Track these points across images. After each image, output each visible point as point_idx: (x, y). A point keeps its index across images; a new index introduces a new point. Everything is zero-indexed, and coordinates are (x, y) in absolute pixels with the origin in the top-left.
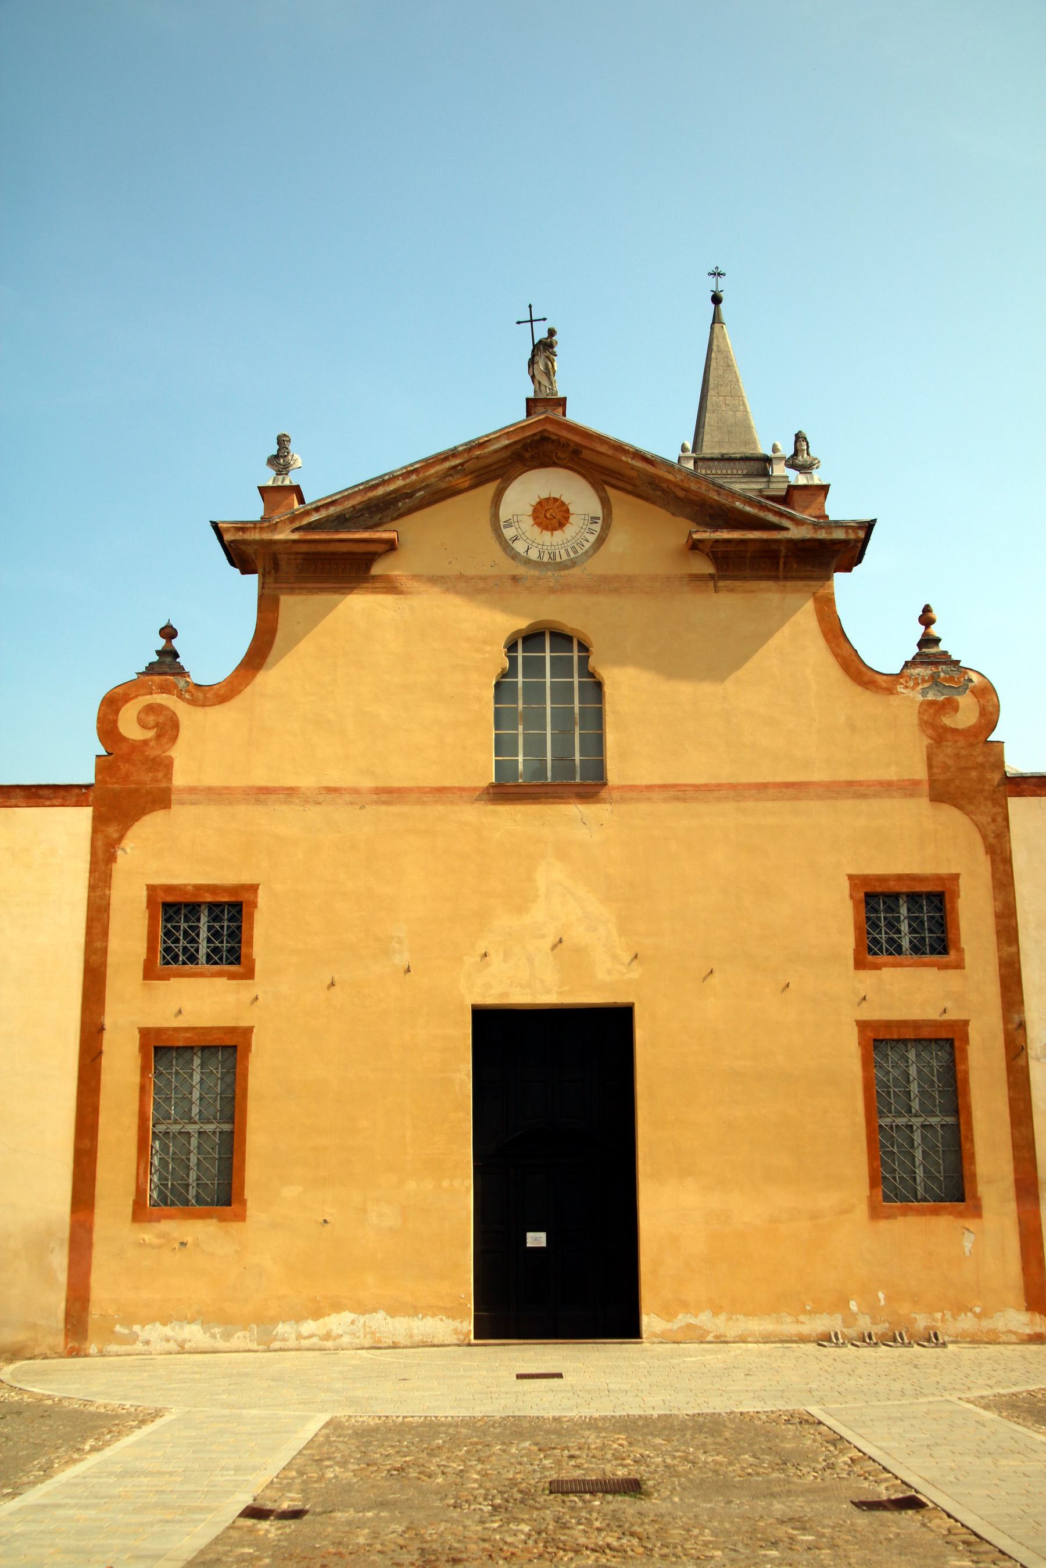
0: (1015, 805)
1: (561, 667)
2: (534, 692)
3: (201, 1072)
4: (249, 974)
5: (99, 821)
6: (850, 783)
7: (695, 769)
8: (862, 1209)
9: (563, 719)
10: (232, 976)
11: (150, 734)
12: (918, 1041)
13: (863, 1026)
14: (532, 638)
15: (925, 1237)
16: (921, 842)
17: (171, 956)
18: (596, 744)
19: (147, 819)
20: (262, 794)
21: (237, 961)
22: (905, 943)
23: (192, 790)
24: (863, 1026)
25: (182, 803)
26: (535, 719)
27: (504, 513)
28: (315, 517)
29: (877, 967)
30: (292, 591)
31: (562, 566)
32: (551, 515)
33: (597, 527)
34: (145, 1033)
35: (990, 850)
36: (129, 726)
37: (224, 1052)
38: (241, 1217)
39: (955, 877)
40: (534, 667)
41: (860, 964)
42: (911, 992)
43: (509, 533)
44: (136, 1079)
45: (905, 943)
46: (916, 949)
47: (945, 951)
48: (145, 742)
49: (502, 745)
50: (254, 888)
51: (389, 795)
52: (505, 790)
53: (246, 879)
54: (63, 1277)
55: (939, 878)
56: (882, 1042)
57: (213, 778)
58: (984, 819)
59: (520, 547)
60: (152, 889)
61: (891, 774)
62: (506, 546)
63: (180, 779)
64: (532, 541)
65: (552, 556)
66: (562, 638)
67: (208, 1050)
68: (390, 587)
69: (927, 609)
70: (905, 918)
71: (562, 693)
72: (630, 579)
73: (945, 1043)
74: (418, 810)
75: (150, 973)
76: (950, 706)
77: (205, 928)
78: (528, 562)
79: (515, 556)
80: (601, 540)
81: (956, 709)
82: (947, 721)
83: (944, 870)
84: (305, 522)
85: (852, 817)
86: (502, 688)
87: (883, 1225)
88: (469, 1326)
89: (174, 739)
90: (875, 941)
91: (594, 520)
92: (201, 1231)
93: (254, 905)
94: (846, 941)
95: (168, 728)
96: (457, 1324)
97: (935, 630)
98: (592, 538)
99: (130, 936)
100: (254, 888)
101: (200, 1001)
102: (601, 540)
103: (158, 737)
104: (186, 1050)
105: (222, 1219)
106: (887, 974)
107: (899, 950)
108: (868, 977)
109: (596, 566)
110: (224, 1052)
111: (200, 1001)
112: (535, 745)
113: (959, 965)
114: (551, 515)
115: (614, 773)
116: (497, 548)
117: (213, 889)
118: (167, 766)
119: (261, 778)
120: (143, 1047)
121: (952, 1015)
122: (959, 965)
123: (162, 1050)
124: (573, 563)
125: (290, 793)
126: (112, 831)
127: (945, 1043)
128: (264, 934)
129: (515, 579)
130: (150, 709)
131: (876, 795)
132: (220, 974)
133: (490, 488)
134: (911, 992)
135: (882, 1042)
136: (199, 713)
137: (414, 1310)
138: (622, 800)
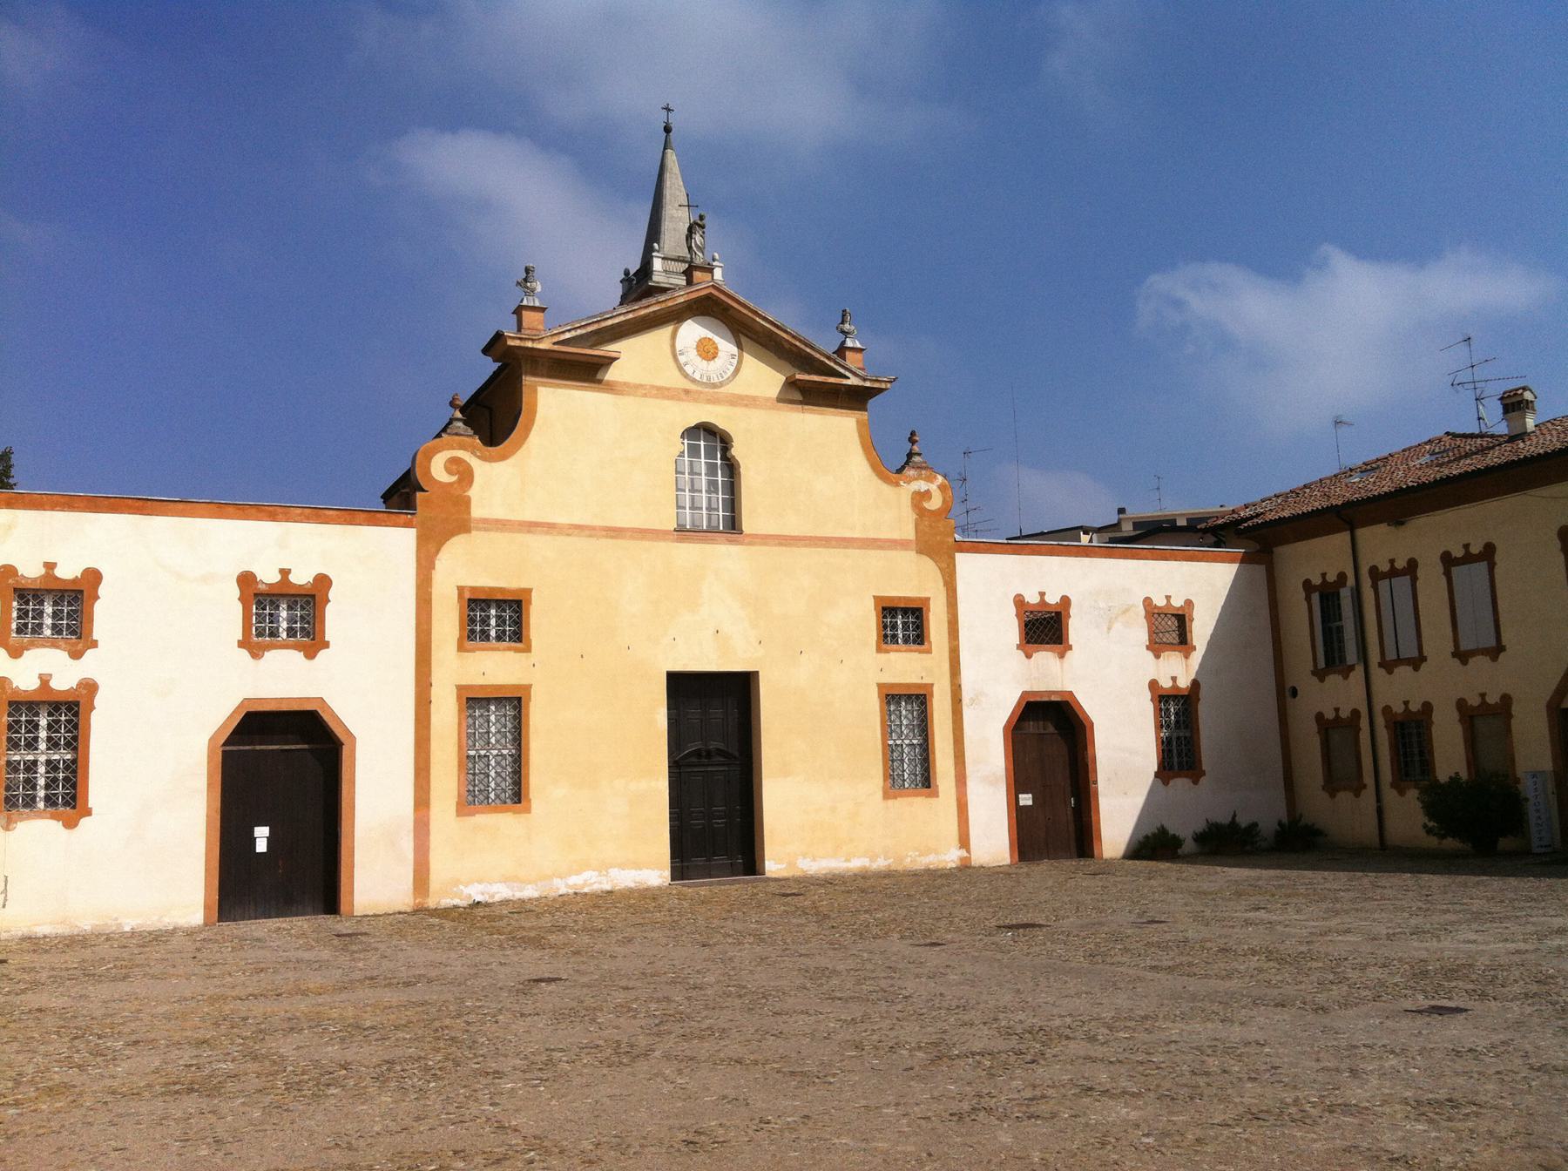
0: (959, 557)
1: (710, 454)
3: (501, 713)
4: (528, 649)
5: (422, 541)
6: (875, 540)
8: (880, 794)
10: (517, 650)
11: (454, 478)
12: (909, 697)
13: (880, 686)
15: (914, 806)
16: (912, 578)
17: (471, 635)
19: (455, 540)
20: (531, 527)
21: (520, 640)
22: (493, 633)
23: (485, 521)
24: (880, 686)
25: (478, 529)
27: (679, 347)
28: (568, 335)
29: (887, 652)
30: (544, 385)
31: (714, 386)
32: (707, 351)
33: (735, 361)
34: (460, 688)
35: (946, 584)
37: (514, 703)
38: (528, 810)
39: (928, 599)
41: (879, 650)
42: (905, 667)
43: (682, 359)
44: (456, 720)
45: (493, 633)
46: (906, 641)
47: (922, 643)
48: (451, 484)
50: (529, 591)
51: (614, 532)
52: (683, 532)
53: (524, 585)
54: (410, 856)
55: (920, 599)
56: (893, 697)
57: (499, 513)
58: (944, 565)
59: (688, 369)
60: (461, 589)
61: (896, 536)
62: (680, 369)
63: (477, 512)
64: (698, 367)
65: (709, 378)
67: (499, 701)
68: (611, 388)
69: (913, 434)
70: (903, 622)
71: (712, 470)
72: (754, 399)
73: (919, 699)
74: (632, 543)
75: (461, 648)
77: (498, 616)
78: (694, 381)
79: (686, 376)
80: (737, 370)
81: (930, 498)
82: (926, 505)
83: (923, 595)
84: (562, 337)
85: (875, 558)
87: (890, 802)
88: (667, 873)
89: (471, 482)
90: (472, 632)
91: (733, 356)
92: (504, 822)
93: (529, 602)
94: (873, 635)
96: (657, 873)
97: (916, 448)
98: (732, 369)
99: (447, 622)
100: (529, 591)
101: (495, 667)
102: (737, 370)
103: (460, 481)
104: (488, 700)
105: (515, 812)
106: (893, 656)
107: (488, 638)
109: (734, 388)
110: (514, 703)
111: (495, 667)
113: (929, 651)
114: (707, 351)
116: (677, 373)
117: (501, 590)
118: (467, 502)
119: (529, 516)
120: (459, 697)
121: (925, 681)
122: (929, 651)
123: (474, 701)
124: (722, 384)
125: (550, 528)
126: (432, 547)
127: (919, 699)
128: (538, 620)
129: (687, 392)
130: (455, 461)
131: (889, 548)
132: (509, 649)
133: (669, 329)
134: (905, 667)
135: (893, 697)
136: (487, 466)
137: (638, 866)
138: (750, 544)
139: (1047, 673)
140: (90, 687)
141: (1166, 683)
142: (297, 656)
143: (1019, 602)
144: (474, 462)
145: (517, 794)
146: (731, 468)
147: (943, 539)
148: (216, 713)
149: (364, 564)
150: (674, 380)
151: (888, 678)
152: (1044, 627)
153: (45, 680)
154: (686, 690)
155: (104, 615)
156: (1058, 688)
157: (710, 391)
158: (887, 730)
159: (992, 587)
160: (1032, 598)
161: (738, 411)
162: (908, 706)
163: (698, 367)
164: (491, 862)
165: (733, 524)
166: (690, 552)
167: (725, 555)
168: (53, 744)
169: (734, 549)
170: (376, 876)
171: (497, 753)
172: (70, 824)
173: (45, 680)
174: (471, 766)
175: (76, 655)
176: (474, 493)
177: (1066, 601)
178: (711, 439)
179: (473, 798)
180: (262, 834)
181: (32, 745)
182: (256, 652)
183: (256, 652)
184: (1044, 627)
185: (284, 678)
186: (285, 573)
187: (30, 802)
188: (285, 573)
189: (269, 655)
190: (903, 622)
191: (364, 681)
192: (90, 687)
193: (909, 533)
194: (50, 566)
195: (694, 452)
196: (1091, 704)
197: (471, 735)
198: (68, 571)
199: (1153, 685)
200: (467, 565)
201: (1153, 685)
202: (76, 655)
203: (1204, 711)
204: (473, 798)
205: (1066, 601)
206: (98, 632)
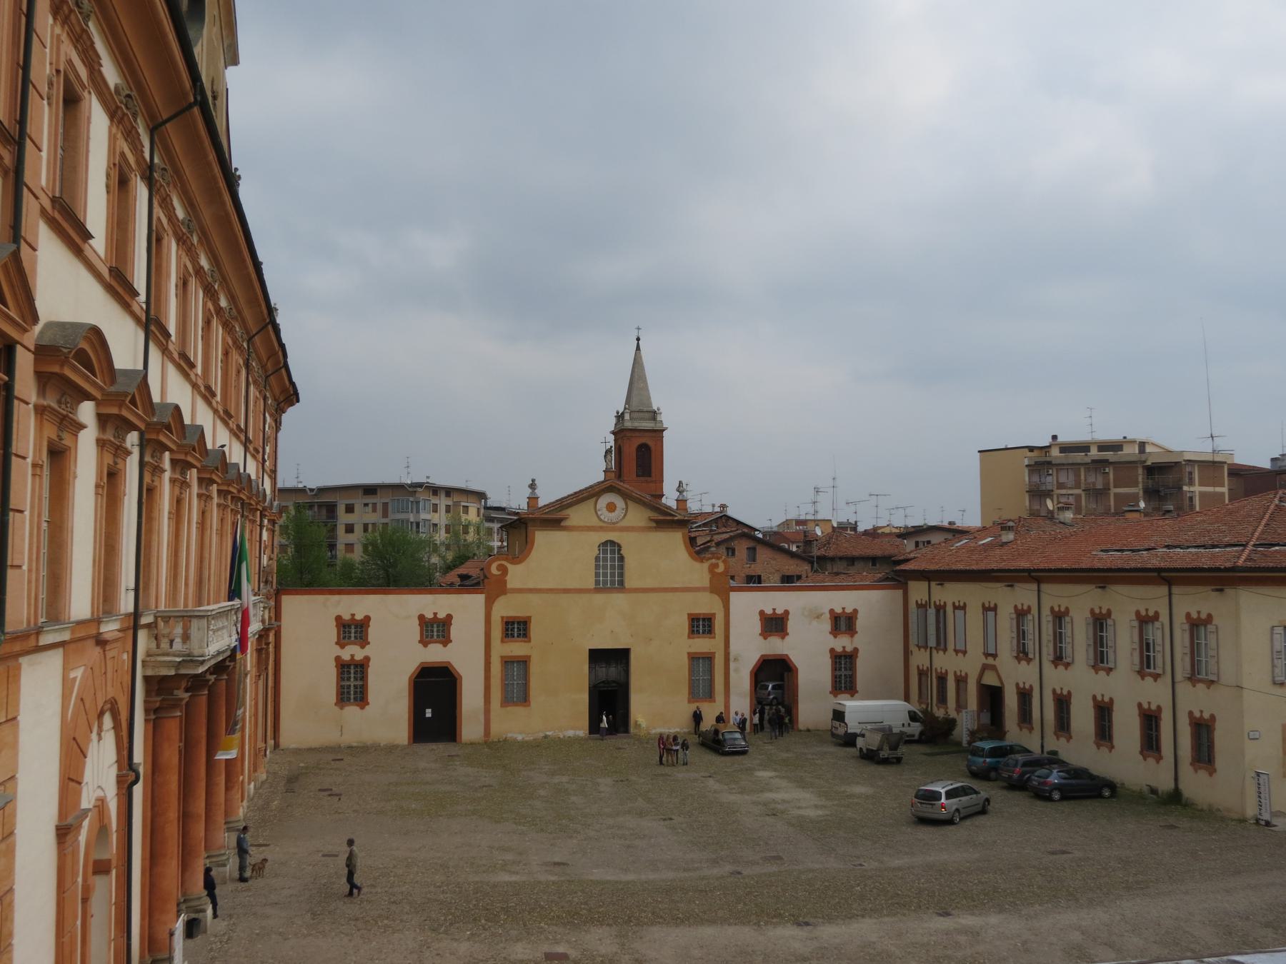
0: (732, 594)
1: (613, 552)
2: (605, 559)
3: (518, 669)
7: (649, 583)
9: (613, 567)
13: (689, 654)
14: (605, 544)
16: (707, 604)
18: (621, 575)
26: (605, 567)
27: (598, 507)
32: (611, 507)
36: (494, 570)
37: (524, 662)
40: (605, 552)
42: (702, 645)
49: (597, 575)
52: (597, 590)
56: (694, 658)
61: (698, 585)
63: (509, 586)
64: (606, 516)
66: (612, 543)
70: (701, 624)
71: (613, 559)
73: (709, 658)
75: (502, 641)
76: (717, 566)
77: (517, 628)
85: (688, 596)
86: (597, 559)
92: (520, 710)
95: (504, 571)
99: (497, 632)
101: (516, 649)
108: (691, 641)
109: (625, 523)
110: (524, 662)
112: (605, 575)
114: (611, 507)
115: (627, 585)
118: (505, 582)
119: (531, 586)
123: (507, 662)
128: (534, 629)
134: (702, 645)
135: (694, 658)
139: (776, 646)
140: (367, 659)
141: (839, 649)
142: (440, 646)
143: (762, 613)
144: (510, 566)
145: (524, 699)
146: (622, 559)
147: (721, 588)
148: (411, 668)
149: (466, 611)
150: (594, 521)
151: (693, 650)
152: (774, 624)
153: (352, 656)
154: (598, 657)
155: (372, 632)
156: (779, 652)
157: (612, 526)
158: (692, 671)
159: (746, 608)
160: (769, 611)
161: (625, 534)
162: (701, 662)
163: (606, 516)
164: (515, 725)
165: (621, 583)
166: (599, 598)
167: (619, 599)
168: (356, 679)
169: (621, 595)
170: (470, 729)
171: (516, 682)
172: (362, 708)
173: (352, 656)
174: (506, 688)
175: (363, 647)
176: (508, 578)
177: (787, 612)
178: (612, 547)
179: (507, 701)
180: (429, 713)
181: (349, 679)
182: (425, 645)
183: (425, 645)
184: (774, 624)
185: (435, 654)
186: (435, 614)
187: (349, 699)
188: (435, 614)
189: (431, 646)
190: (701, 624)
191: (466, 654)
192: (367, 659)
193: (706, 583)
194: (353, 615)
195: (605, 552)
196: (796, 659)
197: (505, 677)
198: (359, 617)
199: (832, 650)
200: (505, 608)
201: (832, 650)
202: (363, 647)
203: (861, 664)
204: (507, 701)
205: (787, 612)
206: (370, 639)
